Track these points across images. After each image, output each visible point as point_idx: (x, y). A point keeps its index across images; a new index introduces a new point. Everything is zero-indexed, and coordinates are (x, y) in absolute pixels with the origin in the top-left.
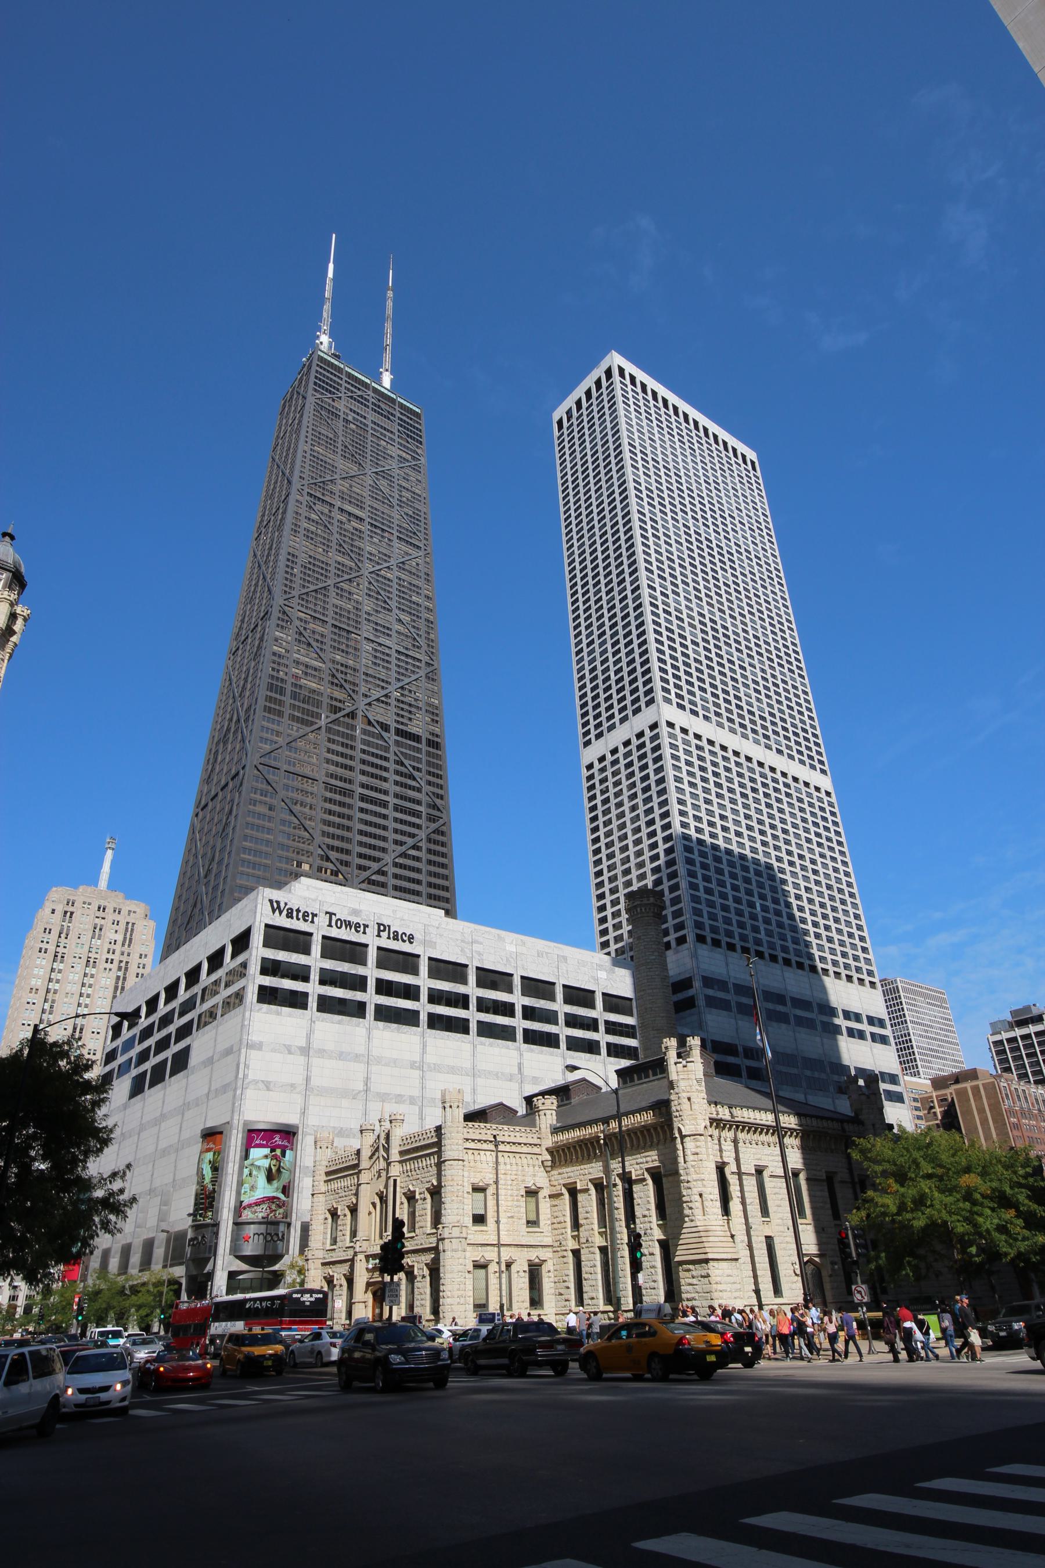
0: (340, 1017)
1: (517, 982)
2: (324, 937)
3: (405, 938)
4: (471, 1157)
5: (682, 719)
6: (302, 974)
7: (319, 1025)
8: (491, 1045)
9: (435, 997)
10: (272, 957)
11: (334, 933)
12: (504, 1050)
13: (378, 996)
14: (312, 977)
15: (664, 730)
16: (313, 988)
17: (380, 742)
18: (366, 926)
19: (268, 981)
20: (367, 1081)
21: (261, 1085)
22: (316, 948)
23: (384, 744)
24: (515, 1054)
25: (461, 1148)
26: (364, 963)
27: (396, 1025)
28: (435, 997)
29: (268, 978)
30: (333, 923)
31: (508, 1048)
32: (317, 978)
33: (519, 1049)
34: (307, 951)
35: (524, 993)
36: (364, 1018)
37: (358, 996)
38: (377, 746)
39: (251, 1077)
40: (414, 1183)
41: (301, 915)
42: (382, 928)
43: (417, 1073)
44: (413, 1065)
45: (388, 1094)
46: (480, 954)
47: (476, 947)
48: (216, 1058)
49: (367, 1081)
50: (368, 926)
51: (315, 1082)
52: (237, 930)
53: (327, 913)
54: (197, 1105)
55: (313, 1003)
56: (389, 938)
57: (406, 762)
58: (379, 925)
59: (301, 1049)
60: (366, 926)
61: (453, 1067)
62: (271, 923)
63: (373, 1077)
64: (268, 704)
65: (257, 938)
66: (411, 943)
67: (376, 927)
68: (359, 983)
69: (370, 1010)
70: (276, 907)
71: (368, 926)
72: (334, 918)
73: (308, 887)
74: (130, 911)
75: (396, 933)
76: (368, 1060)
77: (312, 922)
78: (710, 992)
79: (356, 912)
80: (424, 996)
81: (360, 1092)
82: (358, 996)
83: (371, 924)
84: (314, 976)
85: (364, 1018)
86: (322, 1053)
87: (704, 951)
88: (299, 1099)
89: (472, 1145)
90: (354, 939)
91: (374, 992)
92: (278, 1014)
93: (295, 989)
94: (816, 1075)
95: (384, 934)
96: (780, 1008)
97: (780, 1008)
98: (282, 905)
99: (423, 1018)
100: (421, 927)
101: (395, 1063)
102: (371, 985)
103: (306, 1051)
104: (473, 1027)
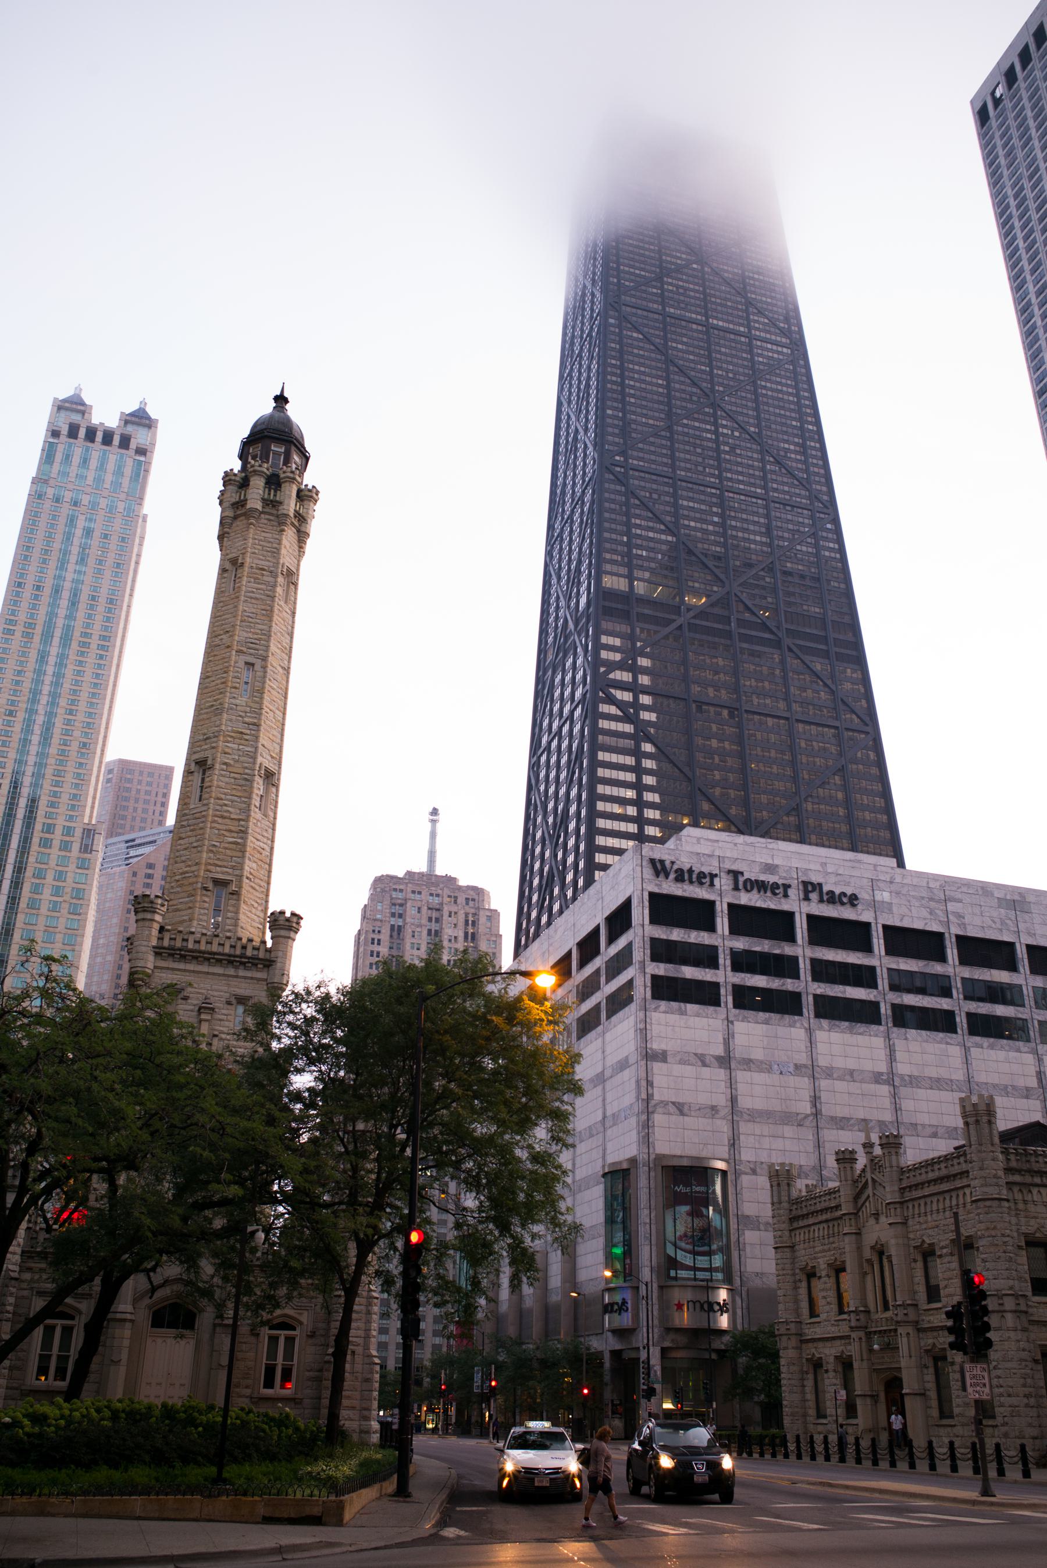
0: (767, 1015)
1: (1021, 953)
2: (730, 905)
3: (845, 900)
4: (1018, 1196)
6: (707, 957)
7: (739, 1027)
8: (991, 1047)
9: (900, 982)
10: (664, 937)
11: (745, 899)
12: (1012, 1054)
13: (816, 985)
14: (721, 961)
16: (724, 976)
17: (767, 636)
18: (787, 887)
19: (661, 969)
20: (815, 1100)
21: (672, 1109)
22: (722, 923)
23: (771, 637)
24: (1029, 1058)
25: (1002, 1182)
26: (791, 938)
27: (847, 1024)
28: (900, 982)
29: (662, 966)
30: (741, 886)
31: (1018, 1051)
32: (728, 962)
33: (1035, 1052)
34: (711, 928)
35: (1034, 971)
36: (801, 1014)
37: (789, 985)
38: (762, 642)
39: (657, 1097)
40: (930, 1232)
41: (694, 876)
42: (810, 888)
43: (885, 1090)
44: (877, 1078)
45: (848, 1119)
46: (959, 916)
47: (951, 907)
48: (608, 1073)
49: (815, 1100)
50: (789, 886)
51: (745, 1102)
52: (613, 903)
53: (729, 872)
54: (592, 1136)
55: (727, 997)
56: (821, 901)
57: (807, 659)
58: (805, 884)
59: (718, 1058)
60: (787, 887)
61: (938, 1080)
62: (656, 890)
63: (824, 1096)
64: (607, 604)
65: (640, 914)
66: (854, 905)
67: (801, 887)
68: (786, 967)
69: (808, 1004)
70: (659, 868)
71: (789, 886)
72: (741, 879)
73: (699, 839)
74: (467, 899)
75: (831, 893)
76: (811, 1070)
77: (712, 884)
79: (770, 868)
80: (883, 982)
81: (807, 1116)
82: (789, 985)
83: (794, 883)
84: (724, 960)
85: (801, 1014)
86: (748, 1063)
88: (724, 1127)
89: (1017, 1178)
90: (772, 906)
91: (810, 979)
92: (683, 1013)
93: (700, 978)
95: (814, 896)
98: (668, 864)
99: (885, 1010)
100: (866, 883)
101: (851, 1075)
102: (804, 967)
103: (725, 1061)
104: (961, 1021)
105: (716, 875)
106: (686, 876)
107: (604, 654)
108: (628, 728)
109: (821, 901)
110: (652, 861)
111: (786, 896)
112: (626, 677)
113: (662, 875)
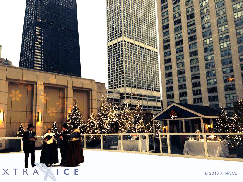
5: (127, 39)
15: (123, 43)
78: (127, 96)
87: (127, 88)
94: (145, 108)
96: (140, 97)
97: (140, 97)
107: (36, 33)
108: (40, 46)
112: (40, 37)
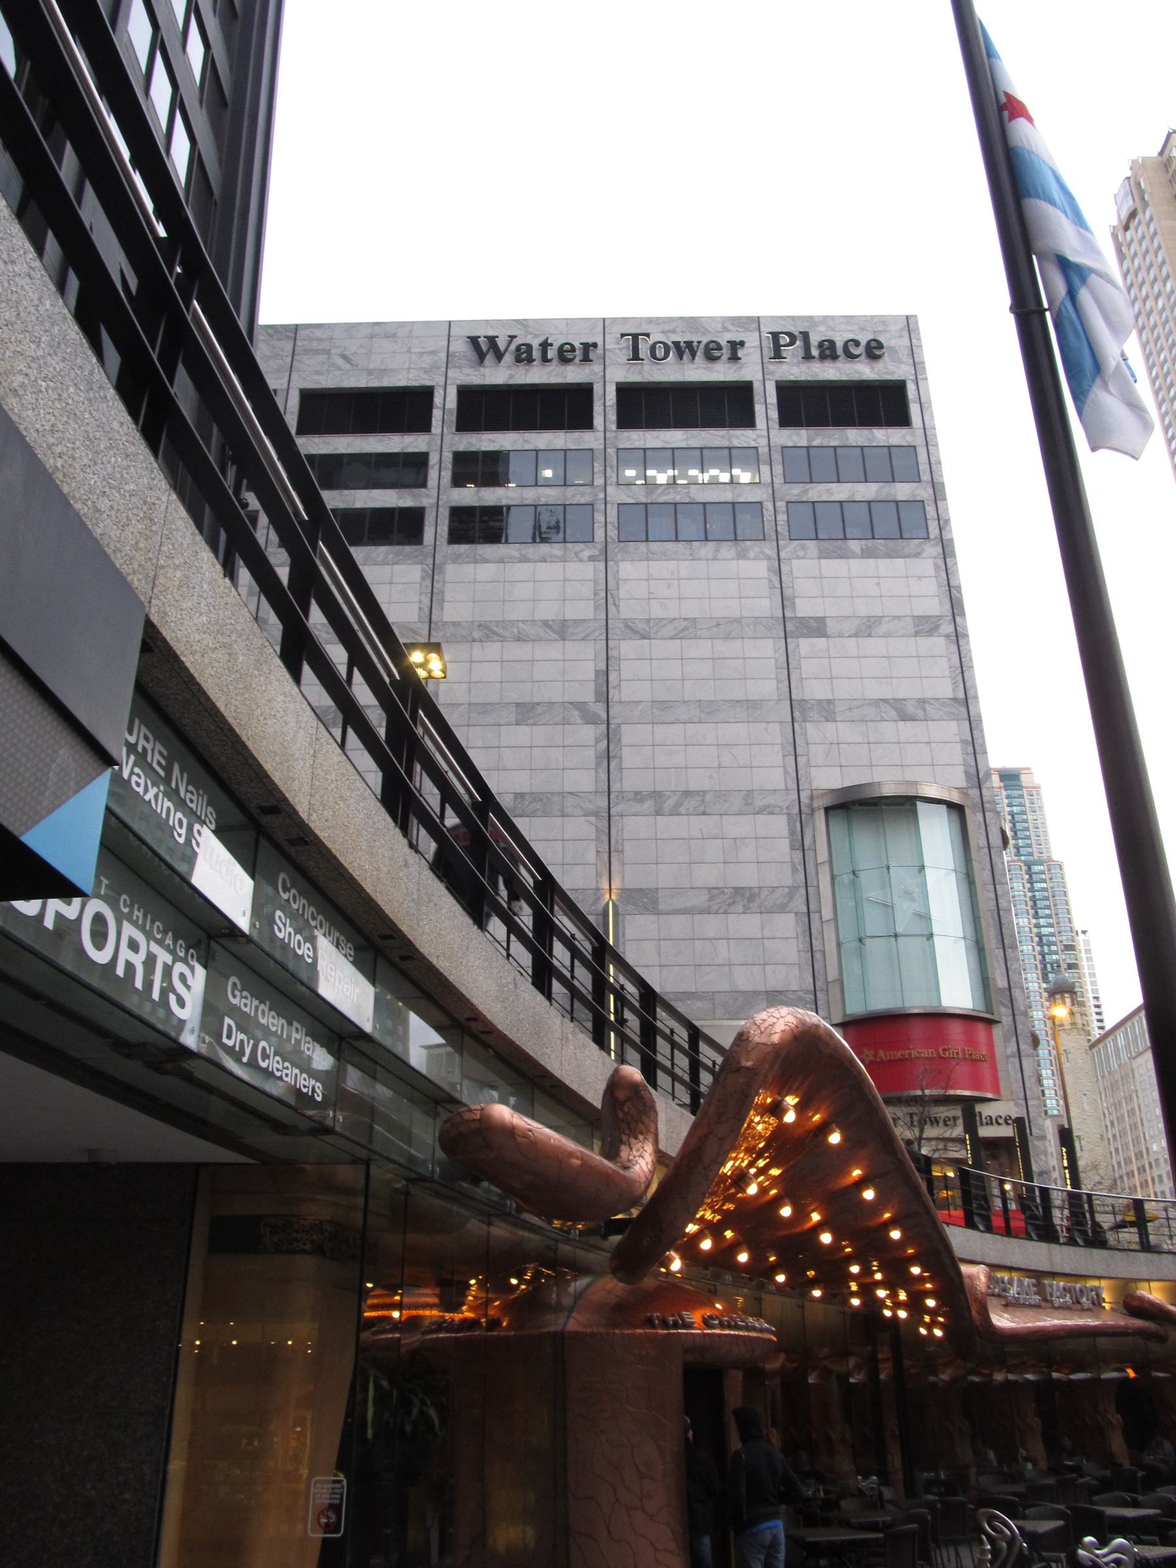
18: (735, 346)
41: (552, 353)
56: (808, 357)
60: (735, 346)
95: (792, 353)
98: (502, 344)
105: (595, 345)
106: (536, 354)
109: (808, 357)
110: (474, 340)
111: (734, 358)
113: (490, 358)
